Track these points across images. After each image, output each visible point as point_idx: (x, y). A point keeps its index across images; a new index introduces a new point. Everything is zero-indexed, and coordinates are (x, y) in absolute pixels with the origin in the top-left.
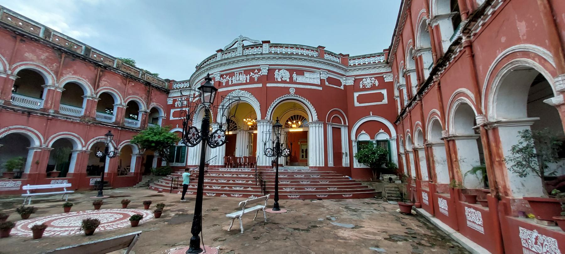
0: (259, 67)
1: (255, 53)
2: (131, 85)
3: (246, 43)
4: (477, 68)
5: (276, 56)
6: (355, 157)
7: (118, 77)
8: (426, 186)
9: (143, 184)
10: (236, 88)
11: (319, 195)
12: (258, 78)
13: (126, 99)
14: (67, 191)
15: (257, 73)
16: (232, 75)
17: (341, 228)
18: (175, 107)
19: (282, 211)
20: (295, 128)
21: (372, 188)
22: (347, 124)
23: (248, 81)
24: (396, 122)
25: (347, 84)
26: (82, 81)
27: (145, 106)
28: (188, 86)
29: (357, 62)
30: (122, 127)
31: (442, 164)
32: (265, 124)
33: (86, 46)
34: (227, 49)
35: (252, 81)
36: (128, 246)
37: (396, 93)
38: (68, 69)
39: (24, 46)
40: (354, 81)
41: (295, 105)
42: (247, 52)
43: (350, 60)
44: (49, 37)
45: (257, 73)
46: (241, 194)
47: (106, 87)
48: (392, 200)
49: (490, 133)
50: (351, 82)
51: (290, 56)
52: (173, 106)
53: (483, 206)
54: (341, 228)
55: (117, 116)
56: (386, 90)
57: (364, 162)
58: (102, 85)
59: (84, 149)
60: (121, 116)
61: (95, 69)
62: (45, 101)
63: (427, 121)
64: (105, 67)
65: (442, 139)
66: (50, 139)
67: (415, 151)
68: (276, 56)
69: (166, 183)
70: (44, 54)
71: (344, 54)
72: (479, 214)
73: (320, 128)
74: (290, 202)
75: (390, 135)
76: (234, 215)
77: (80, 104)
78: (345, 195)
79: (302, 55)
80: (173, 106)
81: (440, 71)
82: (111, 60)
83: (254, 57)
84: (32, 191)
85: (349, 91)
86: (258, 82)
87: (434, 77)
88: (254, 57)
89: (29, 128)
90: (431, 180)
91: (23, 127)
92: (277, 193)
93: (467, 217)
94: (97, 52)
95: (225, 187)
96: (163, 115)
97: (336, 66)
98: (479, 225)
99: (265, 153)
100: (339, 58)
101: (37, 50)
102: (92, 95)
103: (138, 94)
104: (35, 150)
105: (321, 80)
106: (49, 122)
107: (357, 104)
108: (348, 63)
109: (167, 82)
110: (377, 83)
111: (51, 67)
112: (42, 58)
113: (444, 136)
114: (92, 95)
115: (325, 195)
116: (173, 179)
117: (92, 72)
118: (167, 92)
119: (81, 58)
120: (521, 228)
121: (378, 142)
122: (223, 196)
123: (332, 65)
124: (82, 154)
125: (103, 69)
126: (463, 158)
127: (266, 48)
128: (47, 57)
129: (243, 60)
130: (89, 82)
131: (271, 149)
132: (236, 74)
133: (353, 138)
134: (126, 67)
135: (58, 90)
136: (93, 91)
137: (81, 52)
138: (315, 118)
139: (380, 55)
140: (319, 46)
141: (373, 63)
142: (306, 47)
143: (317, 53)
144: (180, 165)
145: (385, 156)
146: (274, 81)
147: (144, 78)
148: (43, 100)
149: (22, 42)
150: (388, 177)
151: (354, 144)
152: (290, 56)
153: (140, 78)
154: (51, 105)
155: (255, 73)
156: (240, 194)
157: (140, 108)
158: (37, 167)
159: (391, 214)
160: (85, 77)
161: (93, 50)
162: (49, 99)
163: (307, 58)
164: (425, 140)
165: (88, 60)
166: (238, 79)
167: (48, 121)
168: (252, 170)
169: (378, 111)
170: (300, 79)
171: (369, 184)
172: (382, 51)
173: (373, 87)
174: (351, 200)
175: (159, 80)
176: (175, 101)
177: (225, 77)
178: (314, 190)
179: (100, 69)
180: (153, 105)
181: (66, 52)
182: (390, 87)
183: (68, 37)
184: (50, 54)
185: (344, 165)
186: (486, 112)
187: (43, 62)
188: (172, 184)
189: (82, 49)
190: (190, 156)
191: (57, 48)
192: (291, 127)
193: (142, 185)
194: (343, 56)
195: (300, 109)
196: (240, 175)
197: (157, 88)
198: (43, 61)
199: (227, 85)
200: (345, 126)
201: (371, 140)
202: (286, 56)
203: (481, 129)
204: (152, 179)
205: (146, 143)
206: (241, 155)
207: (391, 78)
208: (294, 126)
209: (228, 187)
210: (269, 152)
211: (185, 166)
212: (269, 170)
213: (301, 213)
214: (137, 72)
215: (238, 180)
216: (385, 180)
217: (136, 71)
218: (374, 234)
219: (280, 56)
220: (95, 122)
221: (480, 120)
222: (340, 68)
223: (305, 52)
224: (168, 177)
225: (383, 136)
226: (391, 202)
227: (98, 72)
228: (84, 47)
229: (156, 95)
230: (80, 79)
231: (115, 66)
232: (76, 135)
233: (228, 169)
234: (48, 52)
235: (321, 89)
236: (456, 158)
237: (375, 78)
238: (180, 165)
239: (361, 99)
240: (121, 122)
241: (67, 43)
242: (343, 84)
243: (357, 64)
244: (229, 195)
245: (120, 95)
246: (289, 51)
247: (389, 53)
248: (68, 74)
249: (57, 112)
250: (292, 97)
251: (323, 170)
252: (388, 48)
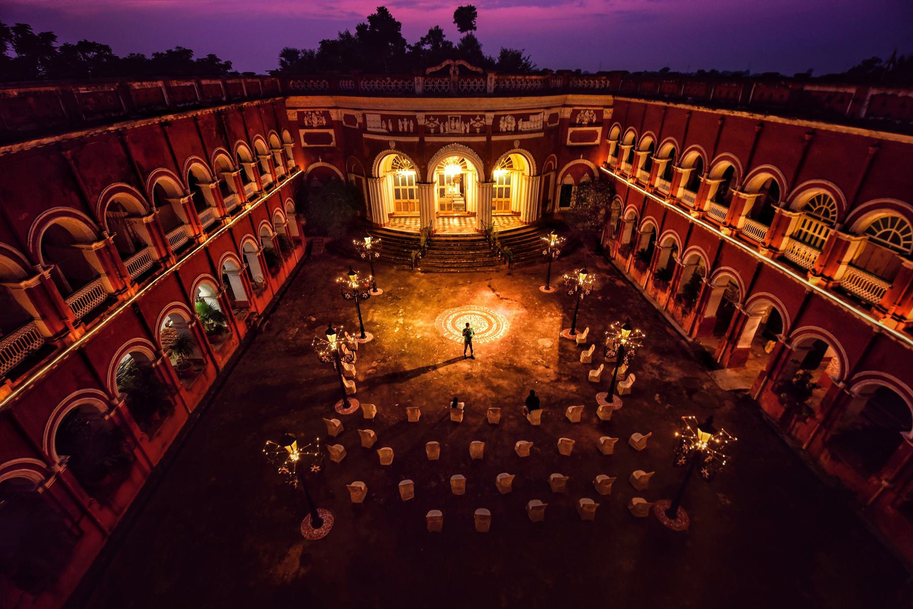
15: (479, 121)
16: (443, 119)
23: (468, 131)
35: (473, 133)
45: (479, 121)
107: (569, 143)
151: (559, 189)
155: (477, 121)
170: (523, 126)
176: (301, 115)
177: (433, 121)
199: (437, 133)
235: (542, 135)
239: (574, 137)
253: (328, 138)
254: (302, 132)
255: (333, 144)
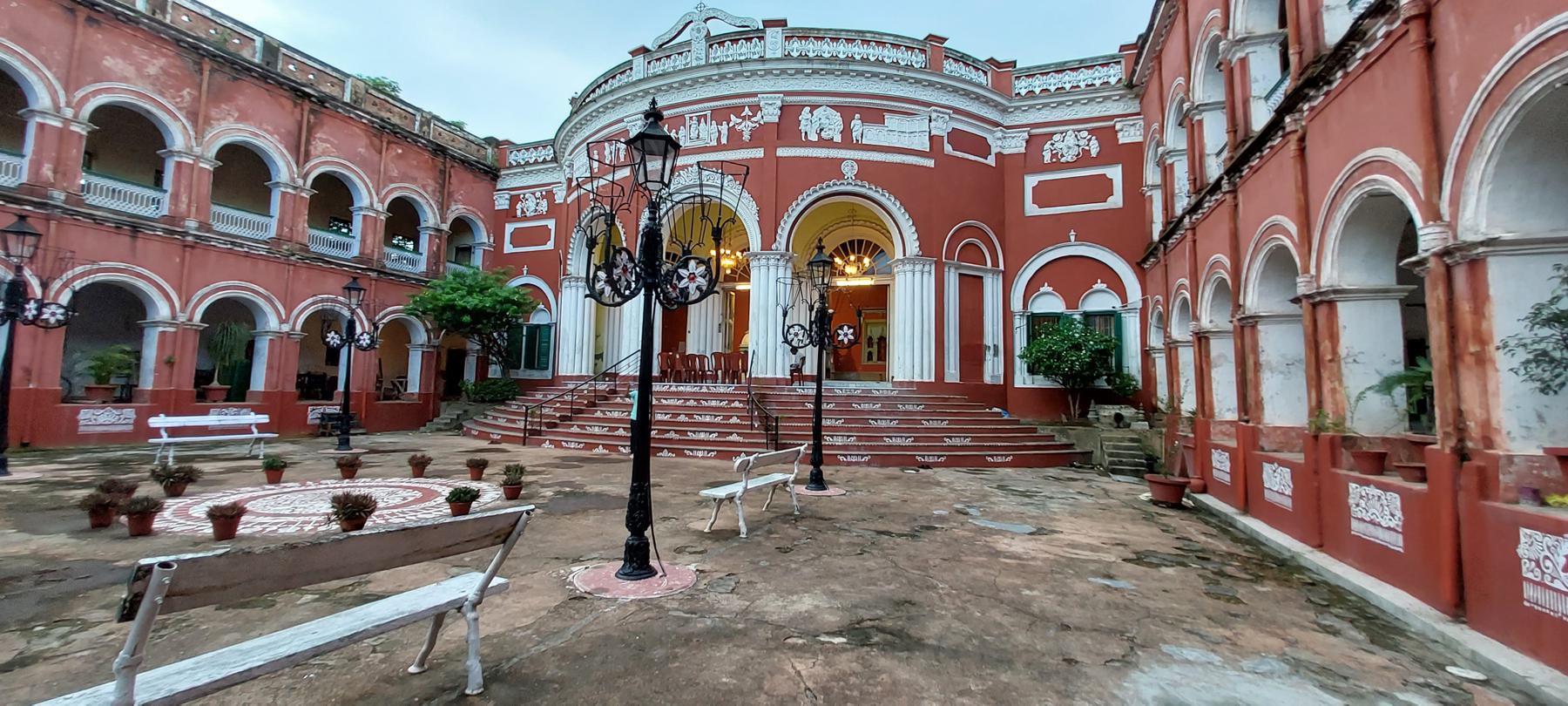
0: (756, 99)
1: (743, 58)
2: (394, 153)
3: (717, 28)
4: (1441, 83)
5: (805, 66)
6: (1021, 357)
7: (358, 131)
8: (1224, 434)
9: (446, 424)
10: (690, 162)
11: (923, 456)
12: (753, 133)
13: (384, 193)
14: (259, 432)
17: (999, 532)
18: (516, 216)
19: (831, 491)
20: (853, 277)
21: (1064, 441)
22: (1002, 267)
23: (724, 141)
24: (1145, 260)
25: (1006, 152)
26: (262, 139)
27: (435, 213)
28: (548, 159)
29: (1037, 84)
30: (380, 272)
31: (1282, 373)
32: (772, 262)
33: (264, 39)
34: (660, 46)
35: (735, 140)
36: (504, 542)
37: (1152, 175)
38: (223, 106)
39: (100, 36)
40: (1027, 142)
41: (851, 210)
42: (719, 54)
43: (1018, 78)
44: (164, 12)
46: (713, 451)
47: (329, 159)
48: (1122, 472)
49: (1461, 277)
50: (1018, 145)
51: (845, 67)
52: (510, 215)
53: (1406, 479)
54: (999, 532)
55: (363, 241)
56: (1120, 167)
57: (1049, 372)
58: (317, 153)
59: (286, 328)
60: (374, 239)
61: (296, 105)
62: (171, 195)
63: (1250, 250)
64: (322, 101)
65: (1297, 300)
66: (195, 299)
67: (1202, 339)
68: (805, 66)
69: (509, 420)
70: (155, 61)
71: (1001, 59)
72: (1395, 500)
73: (926, 275)
74: (845, 472)
75: (1124, 299)
76: (721, 492)
77: (262, 205)
78: (992, 456)
79: (879, 62)
80: (510, 215)
81: (1310, 99)
82: (335, 80)
83: (742, 68)
84: (173, 432)
85: (1009, 169)
86: (754, 142)
87: (1288, 119)
88: (742, 68)
89: (139, 269)
90: (1246, 418)
91: (122, 265)
92: (817, 447)
93: (1353, 508)
94: (296, 56)
95: (668, 431)
96: (486, 241)
97: (978, 97)
98: (1389, 528)
99: (785, 338)
100: (985, 73)
101: (136, 49)
102: (293, 180)
103: (414, 180)
104: (161, 329)
105: (931, 138)
106: (187, 254)
107: (1031, 209)
108: (1010, 86)
109: (489, 144)
110: (1094, 149)
111: (178, 100)
112: (152, 73)
113: (1302, 290)
114: (293, 180)
115: (939, 456)
116: (527, 410)
117: (285, 113)
118: (492, 174)
119: (253, 74)
120: (1523, 531)
121: (1088, 316)
122: (665, 453)
123: (967, 94)
124: (282, 341)
125: (316, 107)
126: (1357, 351)
127: (774, 43)
128: (164, 71)
129: (709, 79)
130: (281, 143)
131: (803, 327)
132: (687, 118)
133: (1017, 304)
134: (377, 101)
135: (202, 165)
136: (295, 170)
137: (253, 56)
138: (913, 247)
139: (1107, 62)
140: (930, 36)
141: (1087, 85)
142: (891, 40)
143: (921, 57)
144: (536, 375)
145: (1110, 352)
146: (798, 140)
147: (429, 133)
148: (166, 191)
149: (91, 26)
150: (1113, 412)
151: (1020, 324)
152: (845, 67)
153: (416, 132)
154: (189, 206)
155: (744, 118)
156: (709, 451)
157: (422, 220)
158: (171, 374)
159: (1126, 504)
160: (269, 128)
161: (284, 50)
162: (182, 190)
163: (895, 72)
164: (1238, 306)
165: (272, 78)
166: (694, 135)
167: (184, 251)
168: (736, 389)
169: (1090, 229)
171: (1059, 431)
172: (1115, 51)
173: (1084, 160)
174: (1009, 470)
175: (470, 141)
176: (514, 200)
178: (909, 442)
179: (307, 106)
180: (457, 209)
181: (214, 56)
182: (1132, 158)
183: (214, 12)
184: (171, 60)
185: (987, 379)
186: (1455, 215)
187: (154, 85)
188: (526, 421)
189: (255, 47)
190: (565, 351)
191: (188, 43)
192: (843, 274)
193: (442, 427)
194: (999, 65)
195: (868, 224)
196: (706, 400)
197: (464, 162)
198: (154, 81)
200: (995, 272)
201: (1069, 312)
202: (833, 67)
203: (1432, 263)
204: (465, 411)
205: (448, 314)
206: (702, 349)
207: (1138, 133)
208: (850, 270)
209: (676, 432)
210: (796, 335)
211: (550, 378)
212: (783, 389)
213: (883, 498)
214: (408, 115)
215: (700, 415)
216: (1102, 420)
217: (404, 114)
218: (1093, 549)
219: (815, 66)
220: (307, 255)
221: (1429, 239)
222: (987, 101)
223: (889, 54)
224: (510, 405)
225: (1100, 301)
226: (1118, 477)
227: (302, 115)
228: (259, 42)
229: (462, 182)
230: (257, 135)
231: (347, 98)
232: (261, 290)
233: (671, 386)
234: (165, 55)
235: (930, 163)
236: (1335, 352)
237: (1091, 131)
238: (536, 375)
239: (1043, 195)
240: (375, 258)
241: (211, 28)
242: (994, 150)
243: (1037, 91)
244: (679, 453)
245: (367, 180)
246: (842, 50)
247: (1139, 55)
248: (224, 119)
249: (204, 226)
250: (849, 188)
251: (933, 392)
252: (1133, 40)
253: (543, 234)
254: (509, 228)
255: (550, 246)
